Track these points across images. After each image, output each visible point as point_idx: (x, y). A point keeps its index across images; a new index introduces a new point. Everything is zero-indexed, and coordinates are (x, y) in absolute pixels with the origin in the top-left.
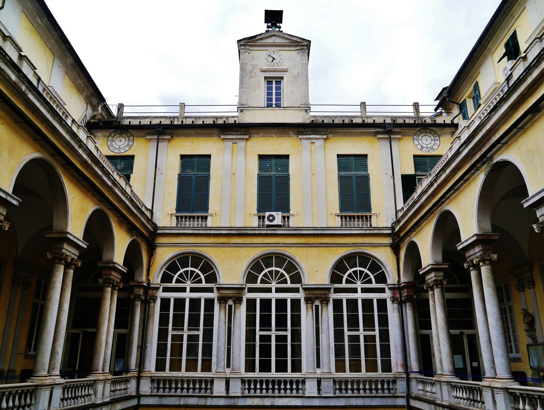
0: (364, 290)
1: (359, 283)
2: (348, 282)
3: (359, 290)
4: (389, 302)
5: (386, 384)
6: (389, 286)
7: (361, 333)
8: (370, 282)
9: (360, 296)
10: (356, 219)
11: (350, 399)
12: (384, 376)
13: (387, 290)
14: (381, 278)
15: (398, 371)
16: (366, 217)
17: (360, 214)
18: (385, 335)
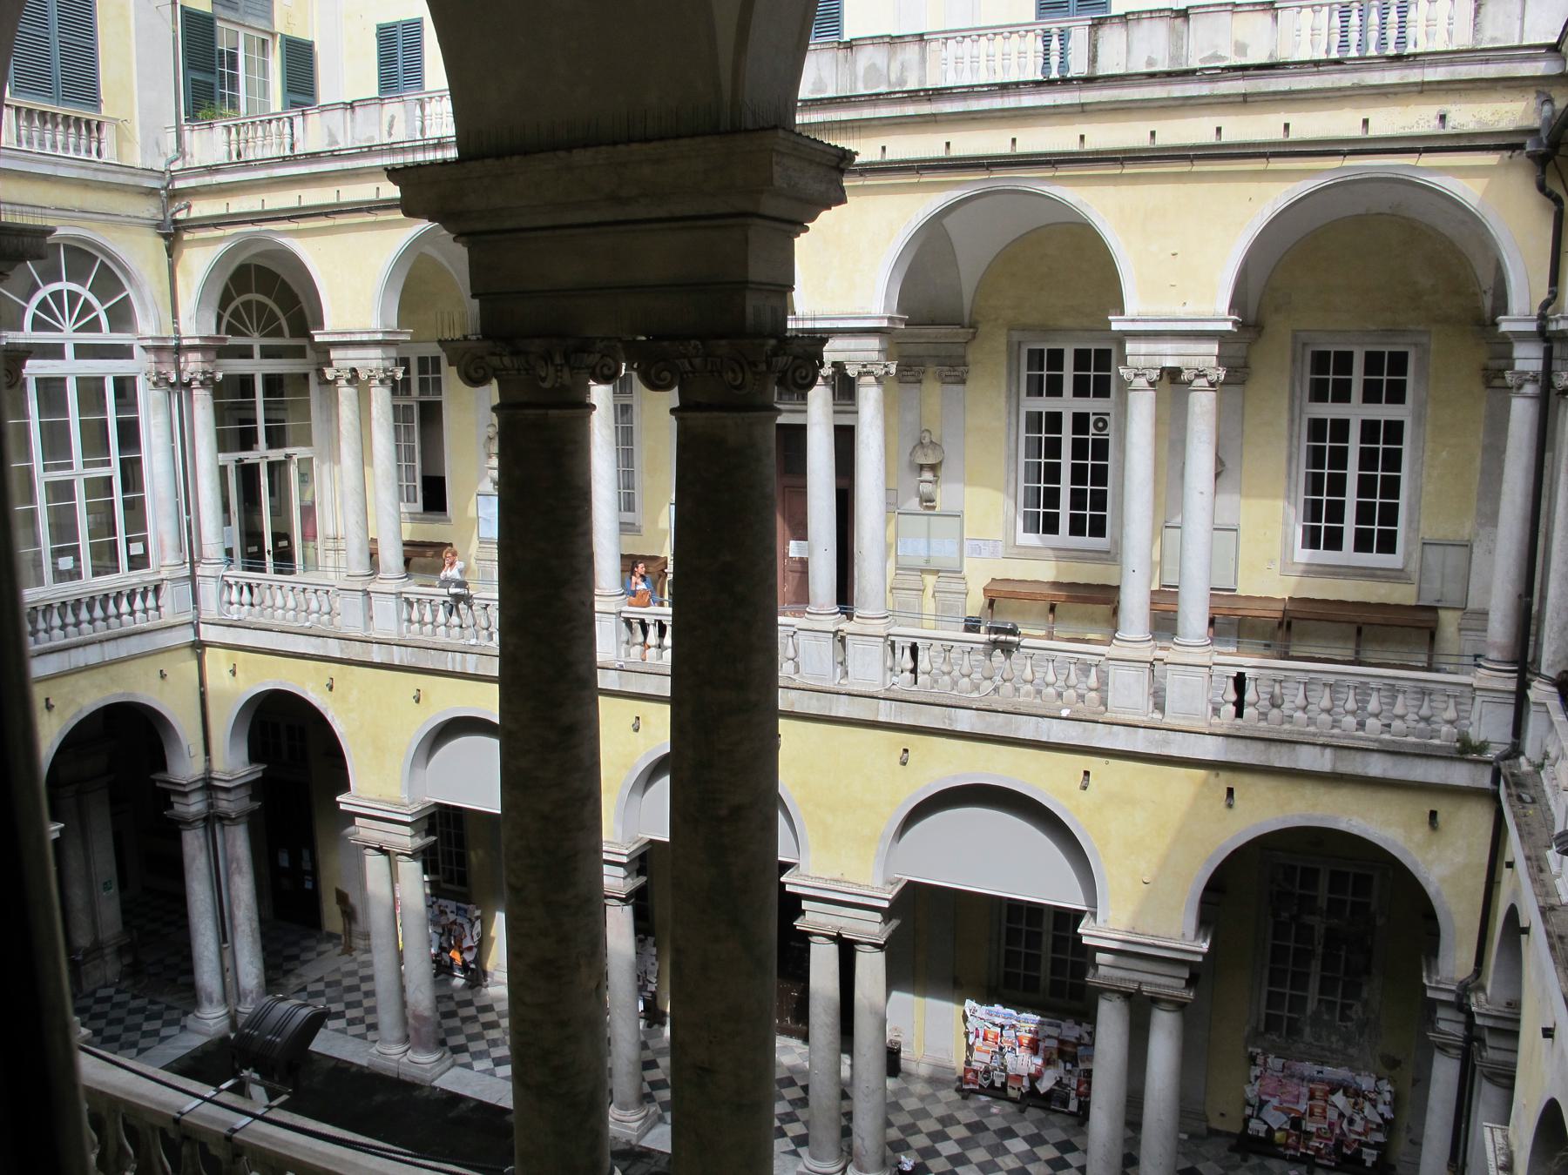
0: (83, 351)
1: (68, 327)
2: (38, 324)
3: (69, 351)
4: (142, 386)
5: (138, 598)
6: (145, 343)
7: (79, 471)
8: (94, 326)
9: (70, 368)
10: (61, 128)
11: (73, 652)
12: (135, 580)
13: (137, 351)
14: (121, 316)
15: (167, 562)
16: (88, 123)
17: (62, 110)
18: (132, 473)
